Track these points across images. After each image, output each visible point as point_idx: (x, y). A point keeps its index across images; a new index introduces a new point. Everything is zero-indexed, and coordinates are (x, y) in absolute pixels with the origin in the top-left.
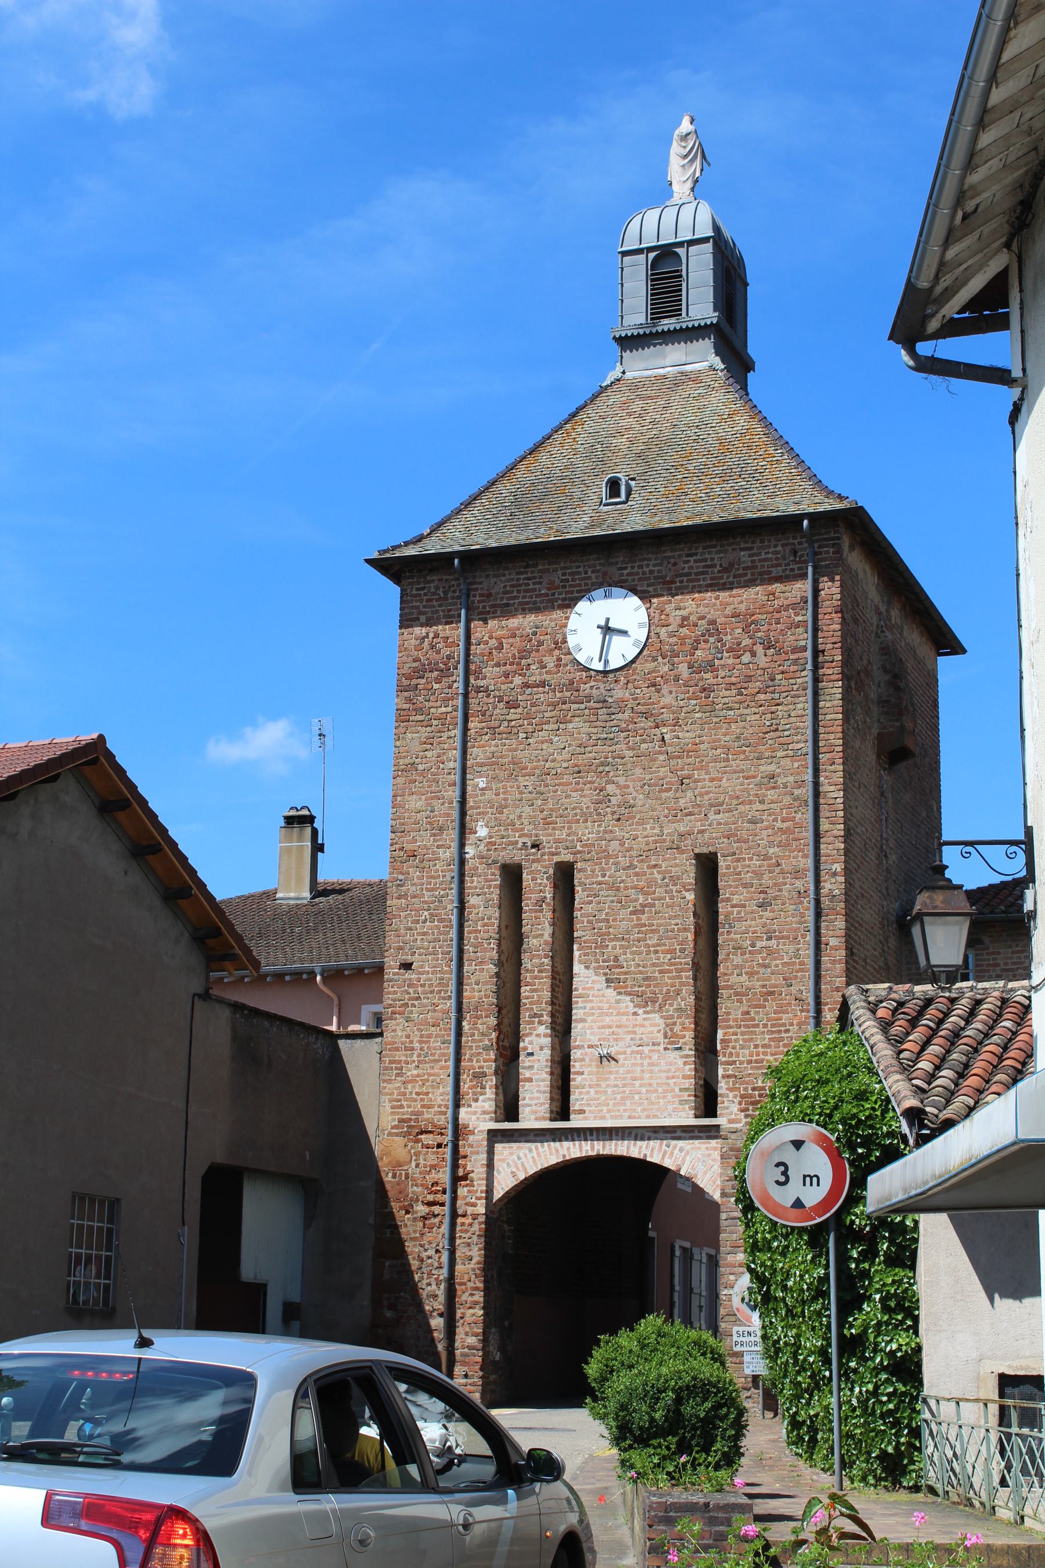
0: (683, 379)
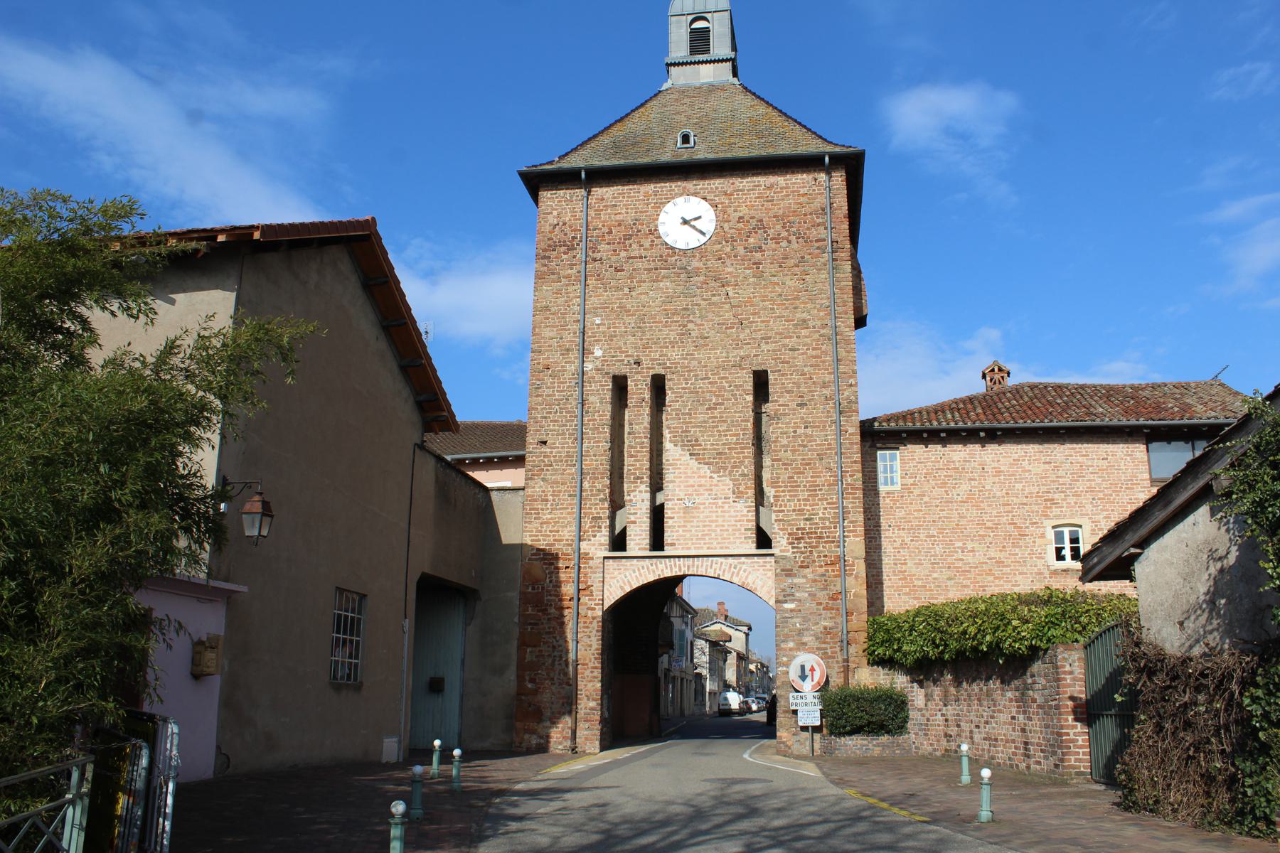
0: (712, 88)
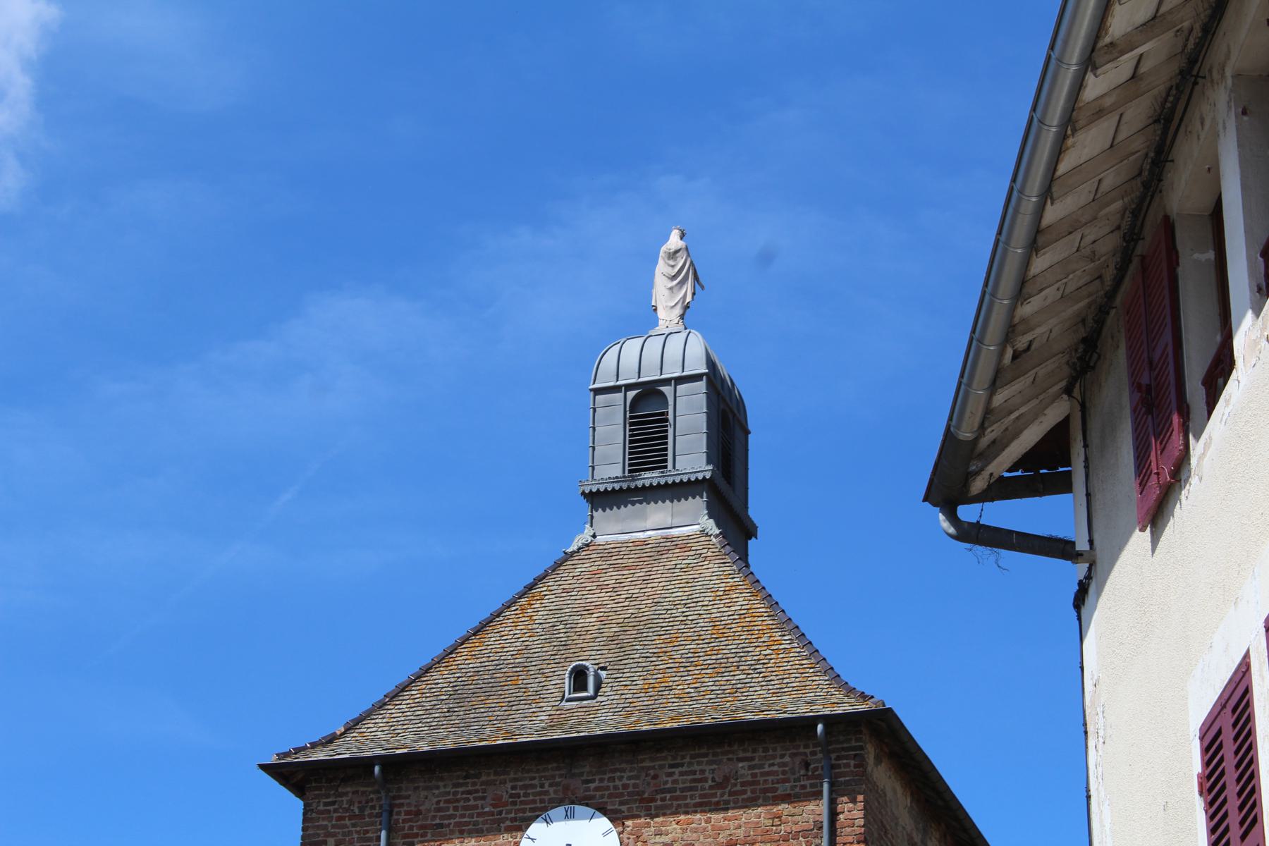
0: (668, 546)
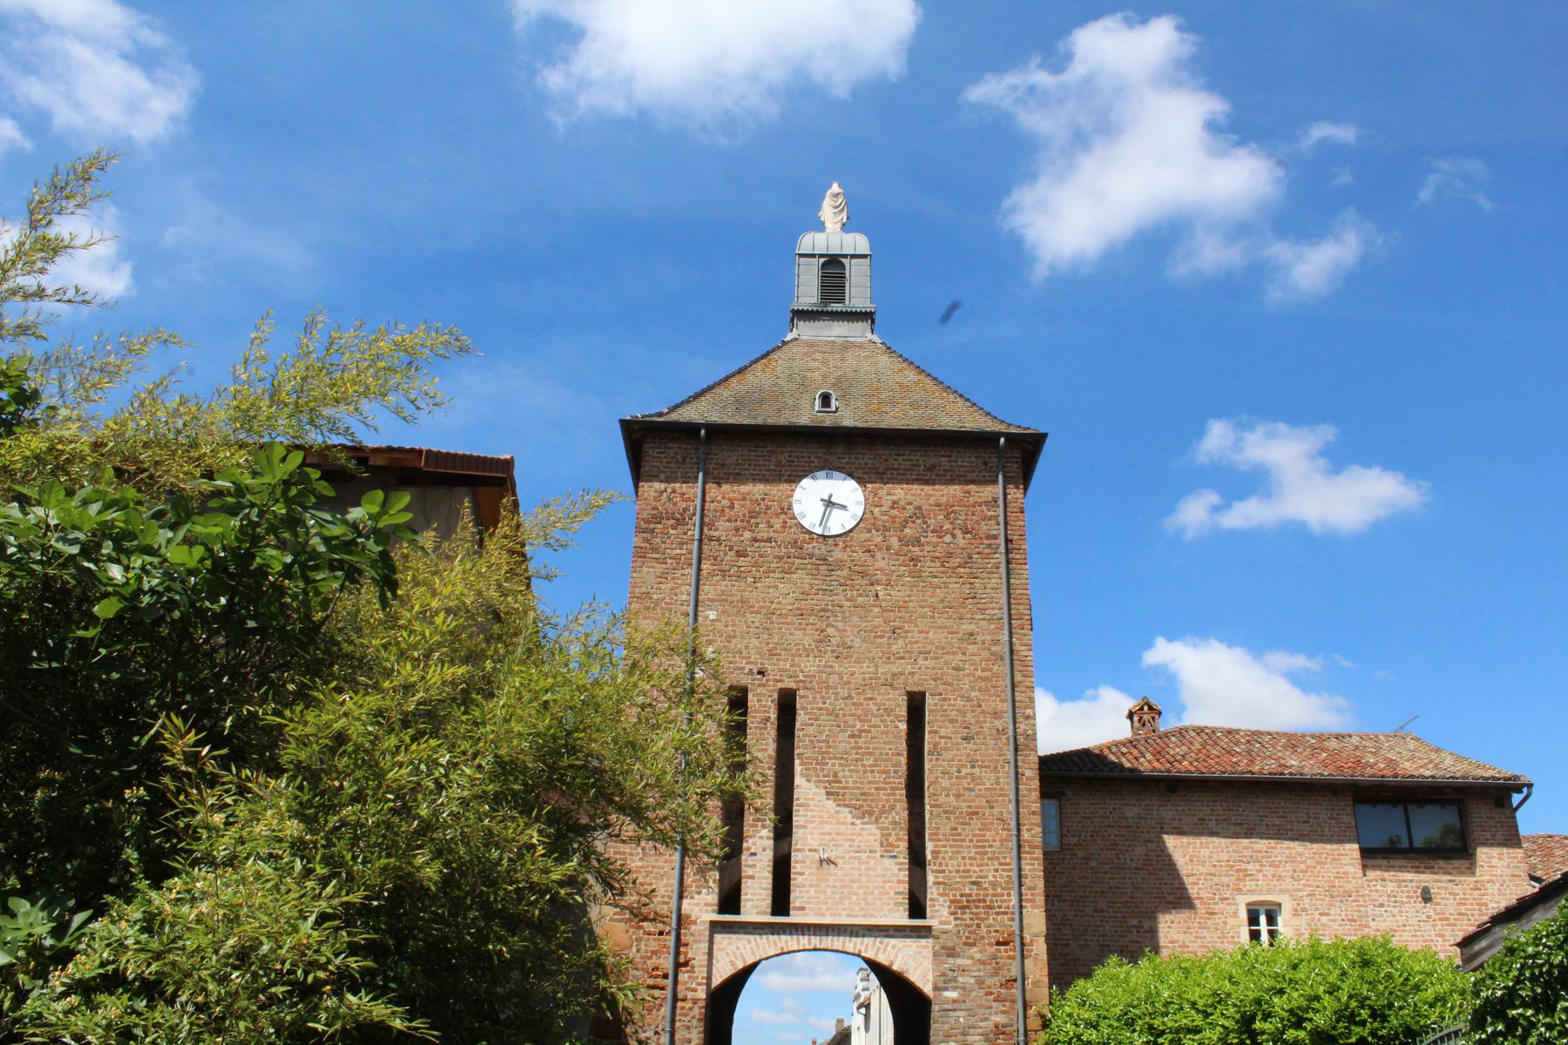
0: (847, 346)
